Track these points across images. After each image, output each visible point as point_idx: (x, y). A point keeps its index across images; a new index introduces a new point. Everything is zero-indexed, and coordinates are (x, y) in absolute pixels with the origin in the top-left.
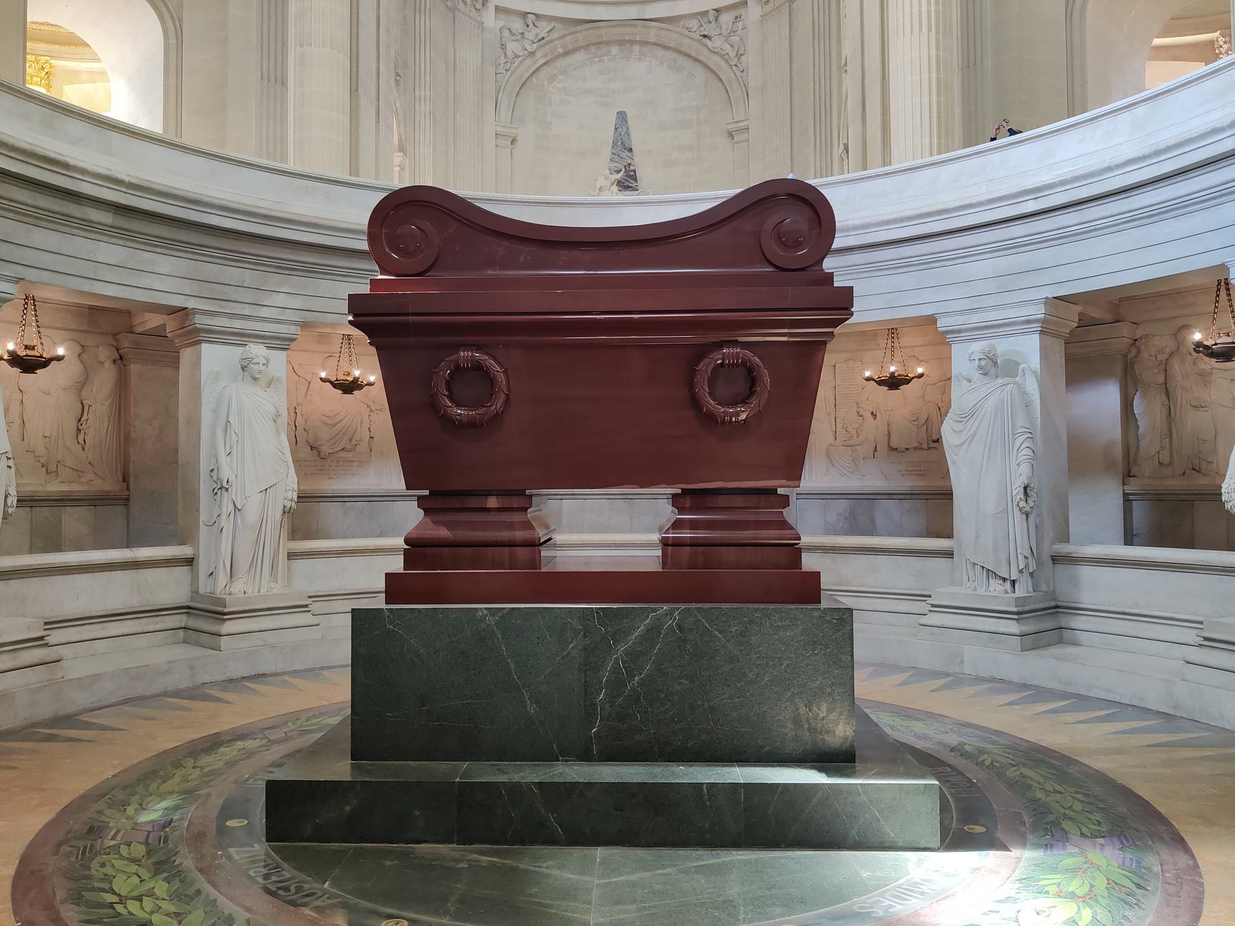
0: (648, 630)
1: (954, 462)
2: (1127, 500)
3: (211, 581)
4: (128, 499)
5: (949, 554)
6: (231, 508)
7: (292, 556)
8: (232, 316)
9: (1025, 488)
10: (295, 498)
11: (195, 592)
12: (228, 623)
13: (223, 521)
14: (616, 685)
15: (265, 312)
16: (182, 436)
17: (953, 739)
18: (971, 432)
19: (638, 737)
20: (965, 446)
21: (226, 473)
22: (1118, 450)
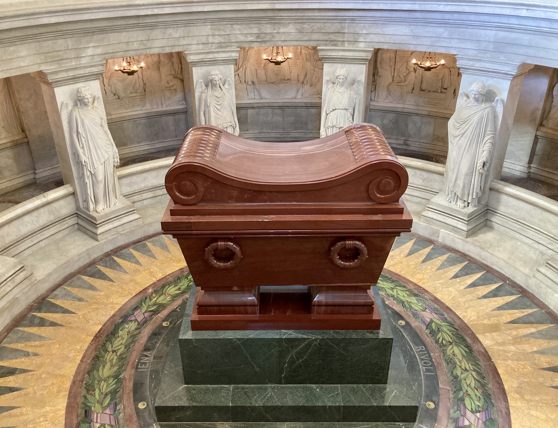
0: (306, 345)
1: (451, 142)
2: (536, 138)
3: (85, 204)
4: (28, 142)
5: (442, 174)
6: (89, 173)
7: (120, 178)
8: (67, 70)
9: (484, 163)
10: (119, 161)
11: (78, 208)
12: (100, 228)
13: (87, 181)
14: (292, 362)
15: (84, 61)
16: (54, 130)
17: (428, 316)
18: (463, 131)
19: (301, 377)
20: (459, 137)
21: (83, 158)
22: (539, 113)
